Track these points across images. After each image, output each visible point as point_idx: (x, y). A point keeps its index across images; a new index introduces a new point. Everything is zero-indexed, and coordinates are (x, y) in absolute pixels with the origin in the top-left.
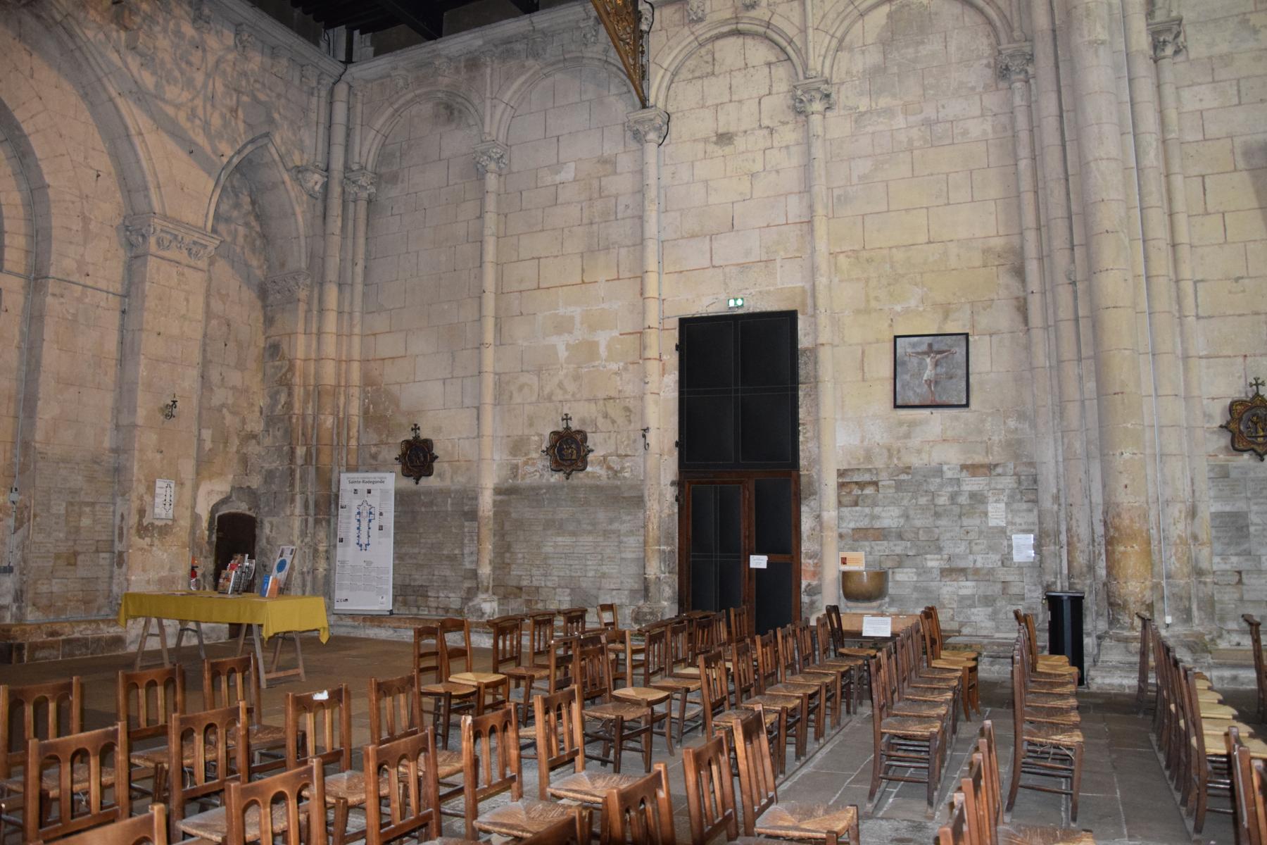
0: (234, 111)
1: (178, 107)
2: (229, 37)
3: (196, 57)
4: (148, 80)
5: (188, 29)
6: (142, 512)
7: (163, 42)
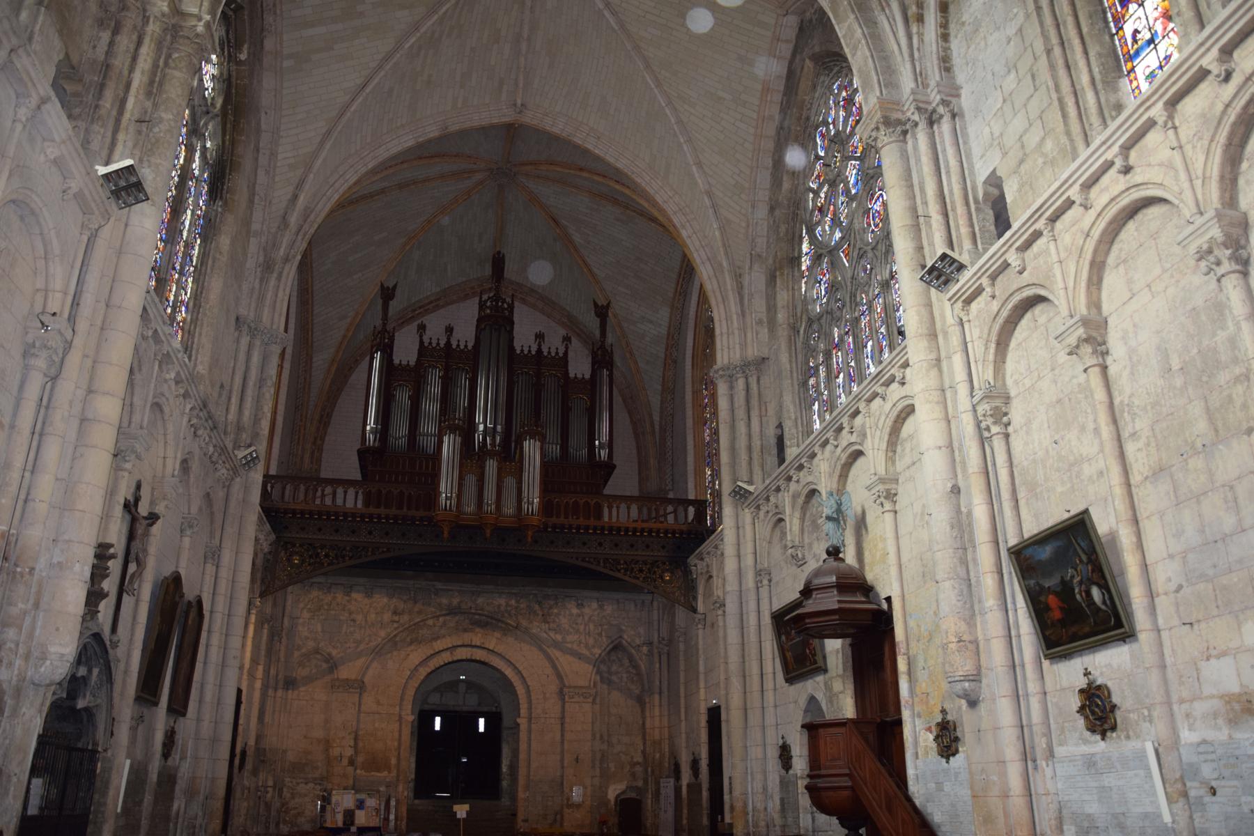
0: (600, 635)
1: (572, 643)
2: (595, 605)
3: (580, 620)
4: (559, 637)
5: (575, 611)
6: (568, 799)
7: (564, 621)
